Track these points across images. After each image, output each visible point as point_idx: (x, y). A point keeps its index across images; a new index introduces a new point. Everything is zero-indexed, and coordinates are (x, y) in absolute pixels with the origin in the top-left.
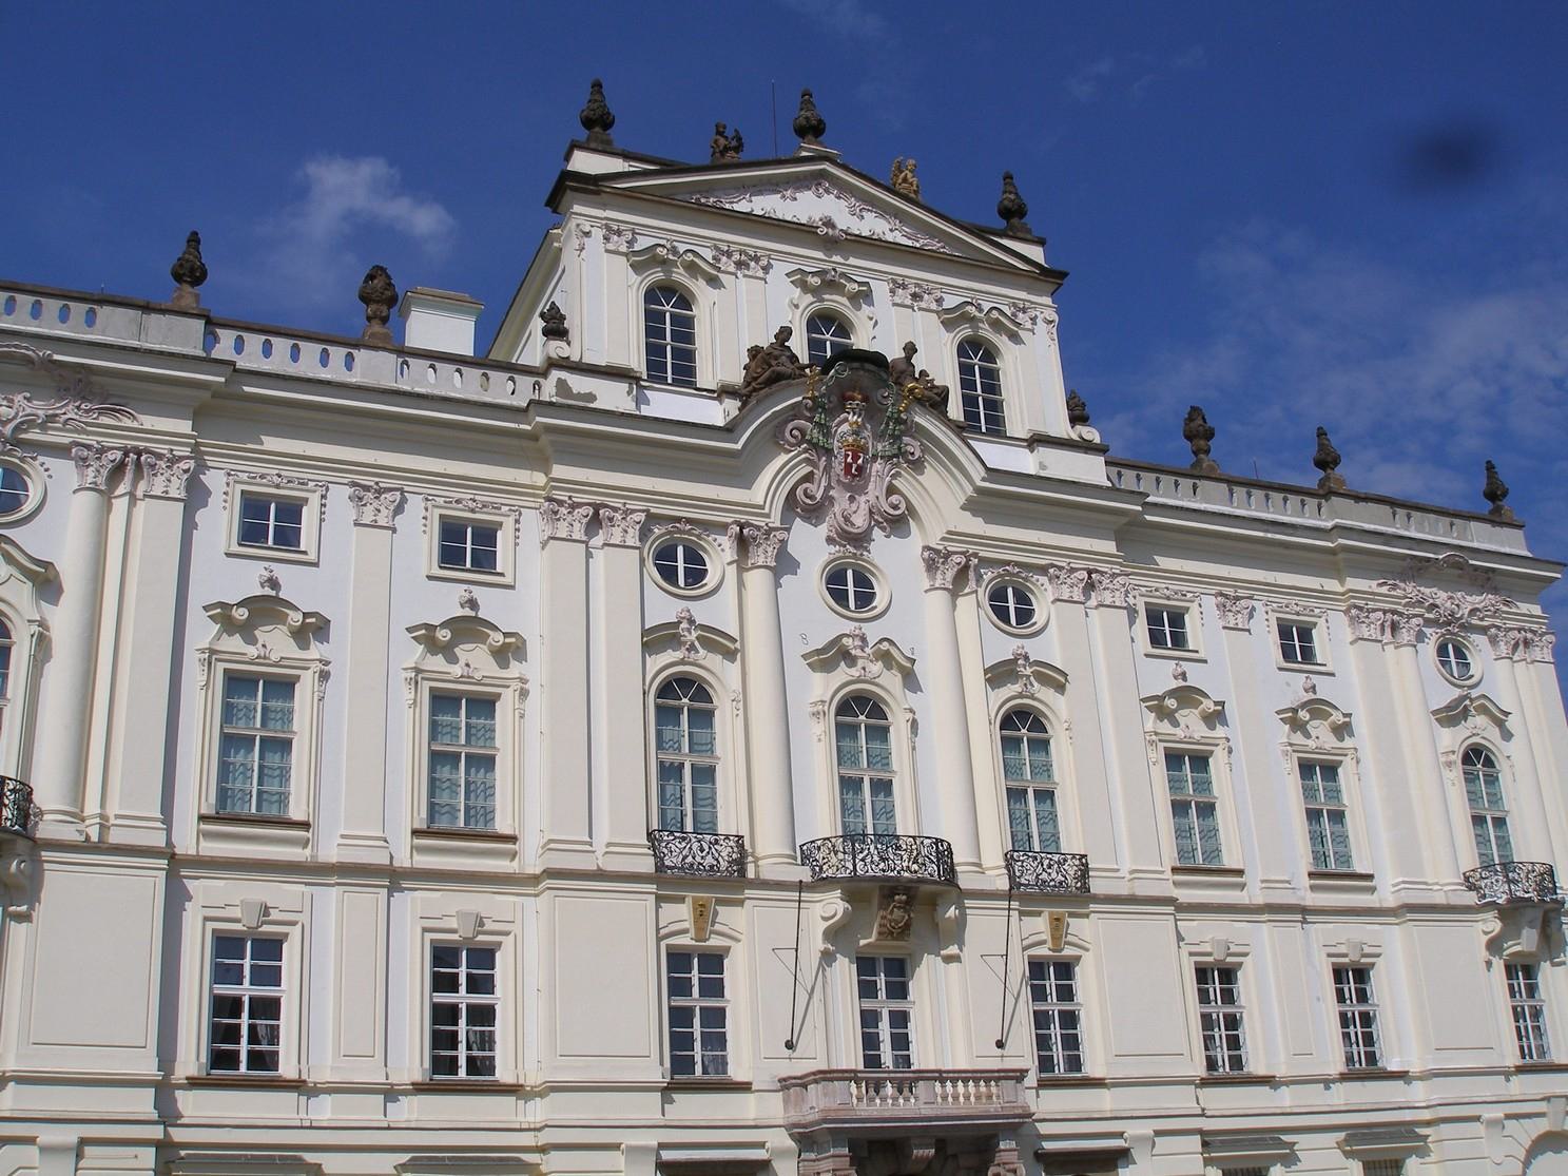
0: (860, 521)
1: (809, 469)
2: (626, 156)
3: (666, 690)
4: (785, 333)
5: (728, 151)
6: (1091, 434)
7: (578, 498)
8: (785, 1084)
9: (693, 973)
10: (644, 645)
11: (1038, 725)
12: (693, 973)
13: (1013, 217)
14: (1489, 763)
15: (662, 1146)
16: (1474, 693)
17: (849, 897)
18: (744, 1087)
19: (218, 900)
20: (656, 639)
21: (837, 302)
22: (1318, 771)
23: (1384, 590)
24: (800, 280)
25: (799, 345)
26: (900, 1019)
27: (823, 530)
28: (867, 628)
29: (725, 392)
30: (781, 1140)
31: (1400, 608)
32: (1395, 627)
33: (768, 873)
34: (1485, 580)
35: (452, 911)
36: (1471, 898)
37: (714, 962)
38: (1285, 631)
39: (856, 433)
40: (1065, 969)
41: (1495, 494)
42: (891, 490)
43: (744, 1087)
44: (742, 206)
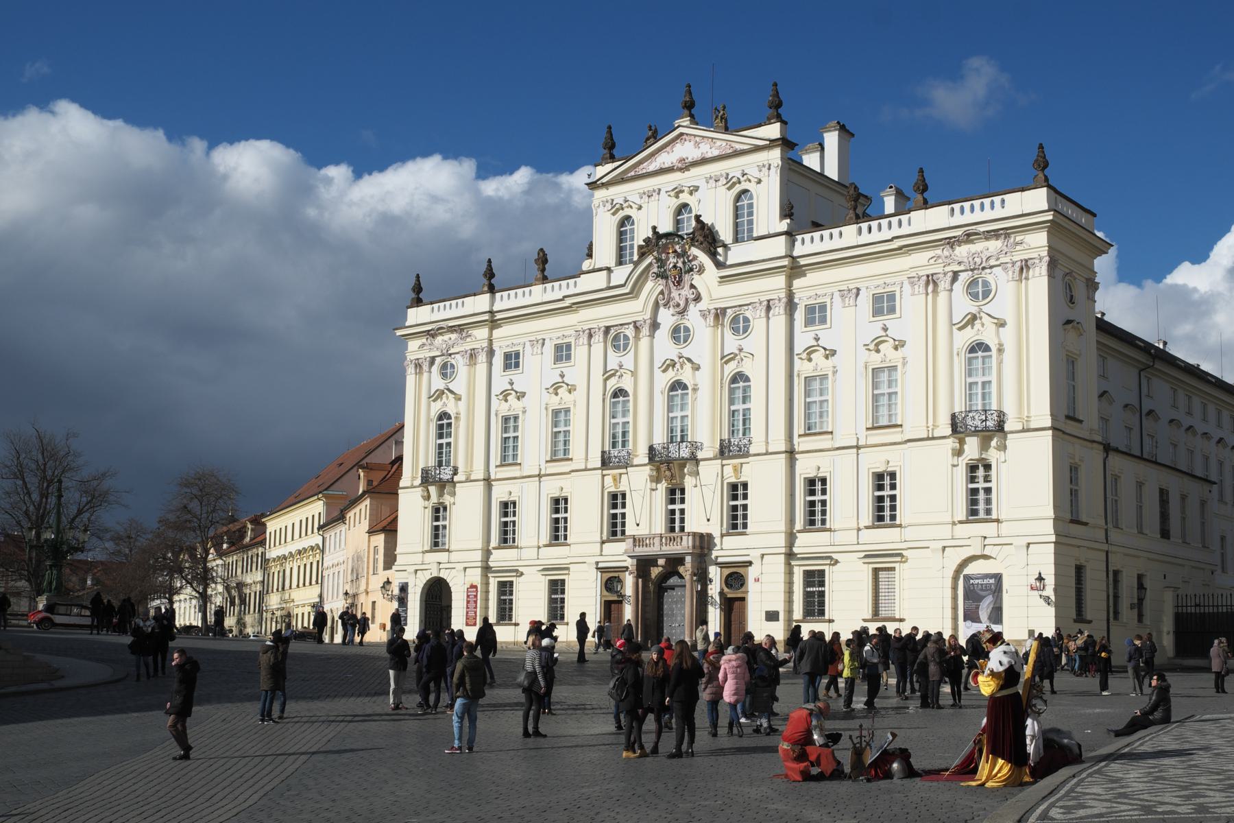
0: (682, 304)
1: (661, 288)
3: (615, 395)
4: (654, 228)
5: (655, 137)
7: (585, 327)
9: (617, 499)
10: (606, 380)
11: (747, 379)
12: (617, 499)
13: (776, 111)
14: (987, 349)
15: (597, 563)
16: (984, 309)
17: (658, 470)
19: (500, 493)
20: (608, 375)
21: (685, 198)
23: (932, 261)
25: (666, 227)
26: (682, 511)
27: (672, 310)
30: (629, 560)
31: (940, 270)
32: (935, 284)
33: (635, 462)
34: (1004, 234)
35: (552, 488)
37: (624, 496)
38: (877, 299)
39: (675, 266)
40: (745, 486)
42: (692, 286)
43: (623, 541)
44: (653, 166)
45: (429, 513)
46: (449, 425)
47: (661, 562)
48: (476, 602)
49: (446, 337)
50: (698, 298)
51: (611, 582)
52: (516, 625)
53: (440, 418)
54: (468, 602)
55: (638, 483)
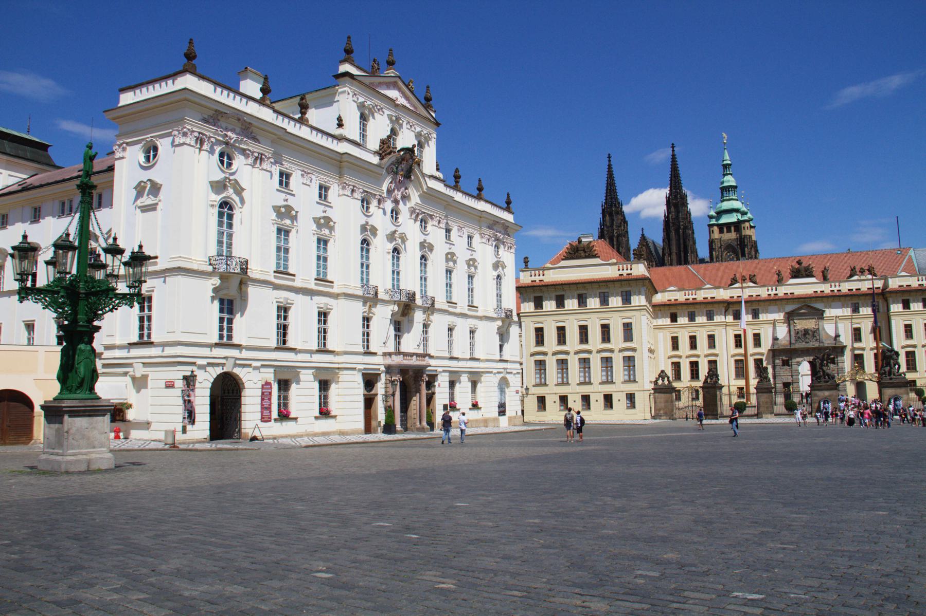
0: (399, 197)
2: (358, 67)
3: (362, 243)
6: (440, 175)
8: (385, 354)
15: (365, 369)
18: (375, 354)
22: (471, 277)
24: (390, 117)
28: (398, 229)
29: (375, 153)
30: (383, 368)
36: (495, 316)
41: (508, 203)
43: (375, 354)
45: (216, 304)
46: (230, 217)
47: (411, 373)
48: (270, 399)
49: (230, 127)
50: (405, 198)
51: (370, 381)
52: (295, 419)
53: (221, 206)
54: (262, 399)
55: (383, 315)
